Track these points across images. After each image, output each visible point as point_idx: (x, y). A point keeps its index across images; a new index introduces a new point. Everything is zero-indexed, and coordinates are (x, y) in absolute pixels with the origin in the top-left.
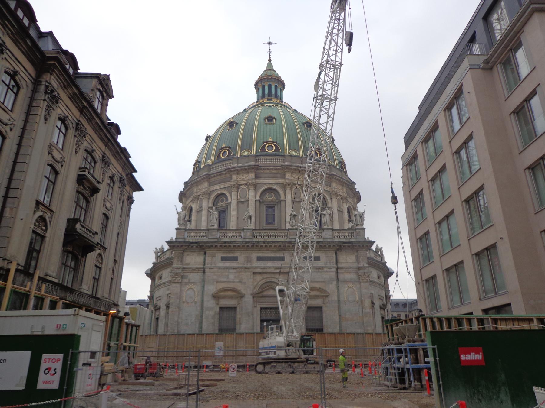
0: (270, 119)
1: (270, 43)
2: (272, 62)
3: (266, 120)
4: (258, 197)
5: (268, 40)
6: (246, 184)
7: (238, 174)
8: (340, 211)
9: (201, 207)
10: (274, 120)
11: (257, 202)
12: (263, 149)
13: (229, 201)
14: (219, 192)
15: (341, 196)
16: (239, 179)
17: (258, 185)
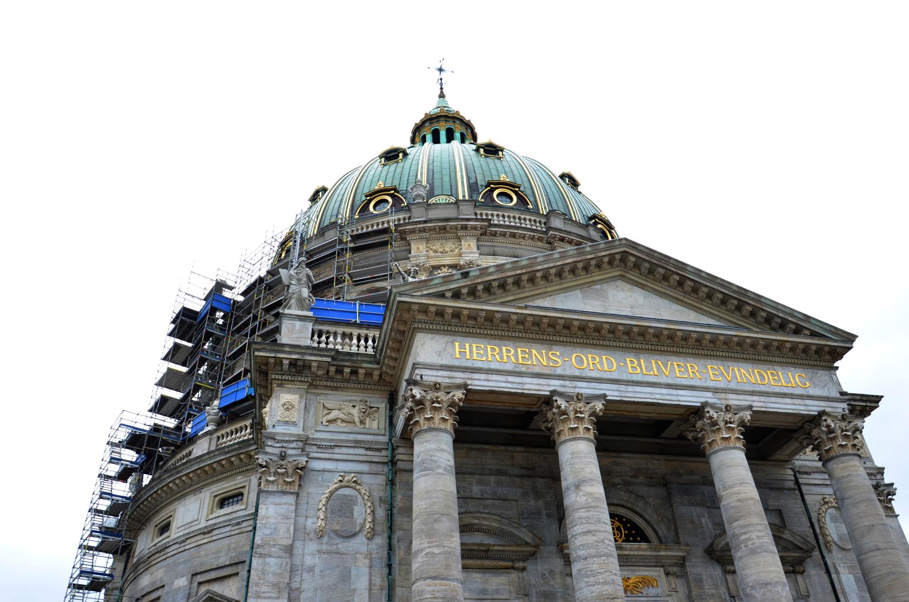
2: (446, 99)
3: (482, 150)
10: (500, 153)
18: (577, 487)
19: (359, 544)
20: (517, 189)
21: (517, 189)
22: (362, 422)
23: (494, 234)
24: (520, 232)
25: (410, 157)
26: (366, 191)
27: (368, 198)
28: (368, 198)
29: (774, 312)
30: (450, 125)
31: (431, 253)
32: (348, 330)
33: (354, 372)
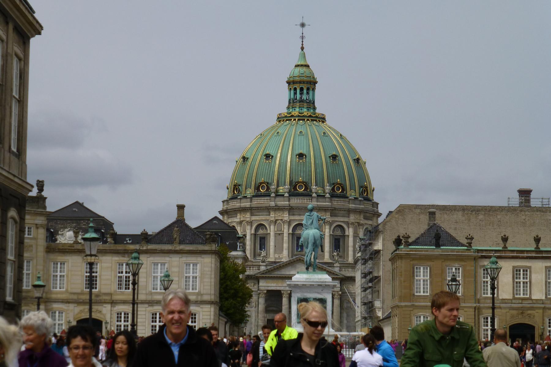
0: (301, 156)
1: (303, 25)
2: (304, 50)
3: (298, 157)
4: (291, 232)
5: (301, 21)
6: (282, 220)
7: (275, 211)
8: (356, 236)
9: (245, 231)
10: (304, 157)
11: (290, 235)
12: (295, 188)
13: (269, 232)
14: (259, 223)
15: (358, 223)
16: (276, 216)
17: (292, 221)
18: (284, 306)
19: (253, 309)
20: (305, 184)
21: (305, 184)
22: (253, 286)
23: (294, 209)
24: (301, 208)
25: (274, 158)
26: (258, 182)
27: (259, 184)
28: (259, 184)
29: (329, 270)
30: (302, 85)
31: (276, 216)
32: (250, 266)
33: (251, 277)
